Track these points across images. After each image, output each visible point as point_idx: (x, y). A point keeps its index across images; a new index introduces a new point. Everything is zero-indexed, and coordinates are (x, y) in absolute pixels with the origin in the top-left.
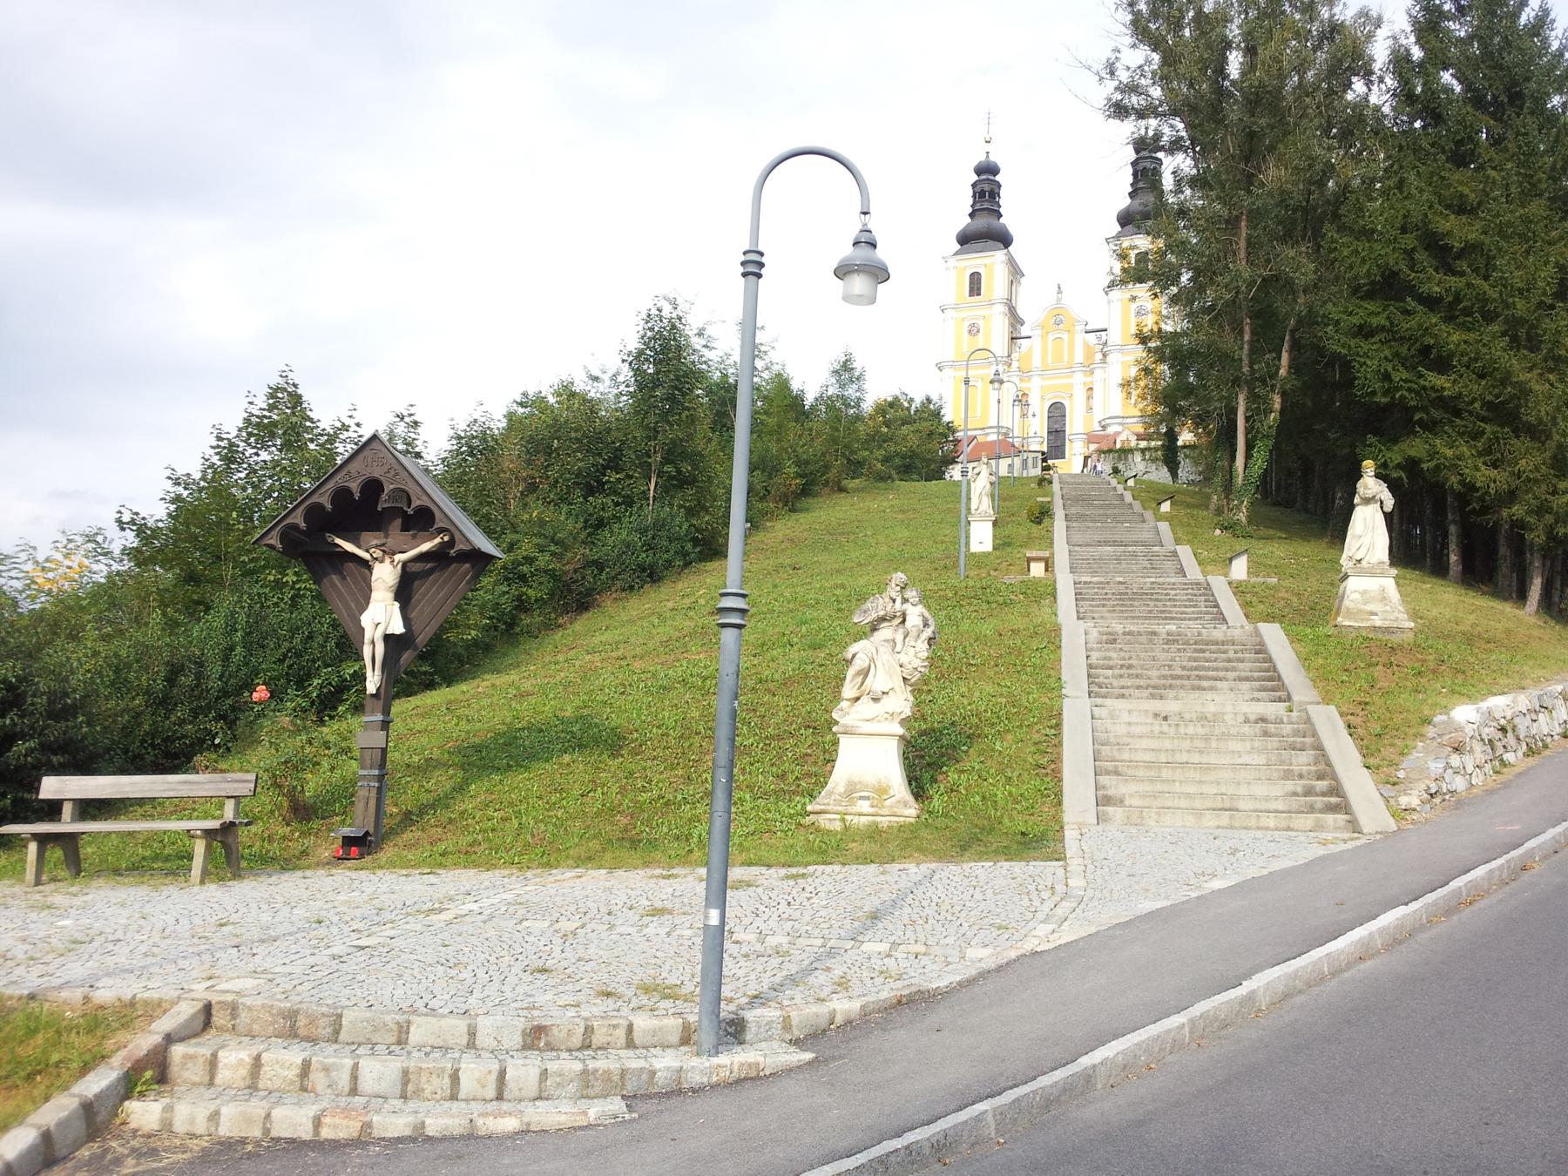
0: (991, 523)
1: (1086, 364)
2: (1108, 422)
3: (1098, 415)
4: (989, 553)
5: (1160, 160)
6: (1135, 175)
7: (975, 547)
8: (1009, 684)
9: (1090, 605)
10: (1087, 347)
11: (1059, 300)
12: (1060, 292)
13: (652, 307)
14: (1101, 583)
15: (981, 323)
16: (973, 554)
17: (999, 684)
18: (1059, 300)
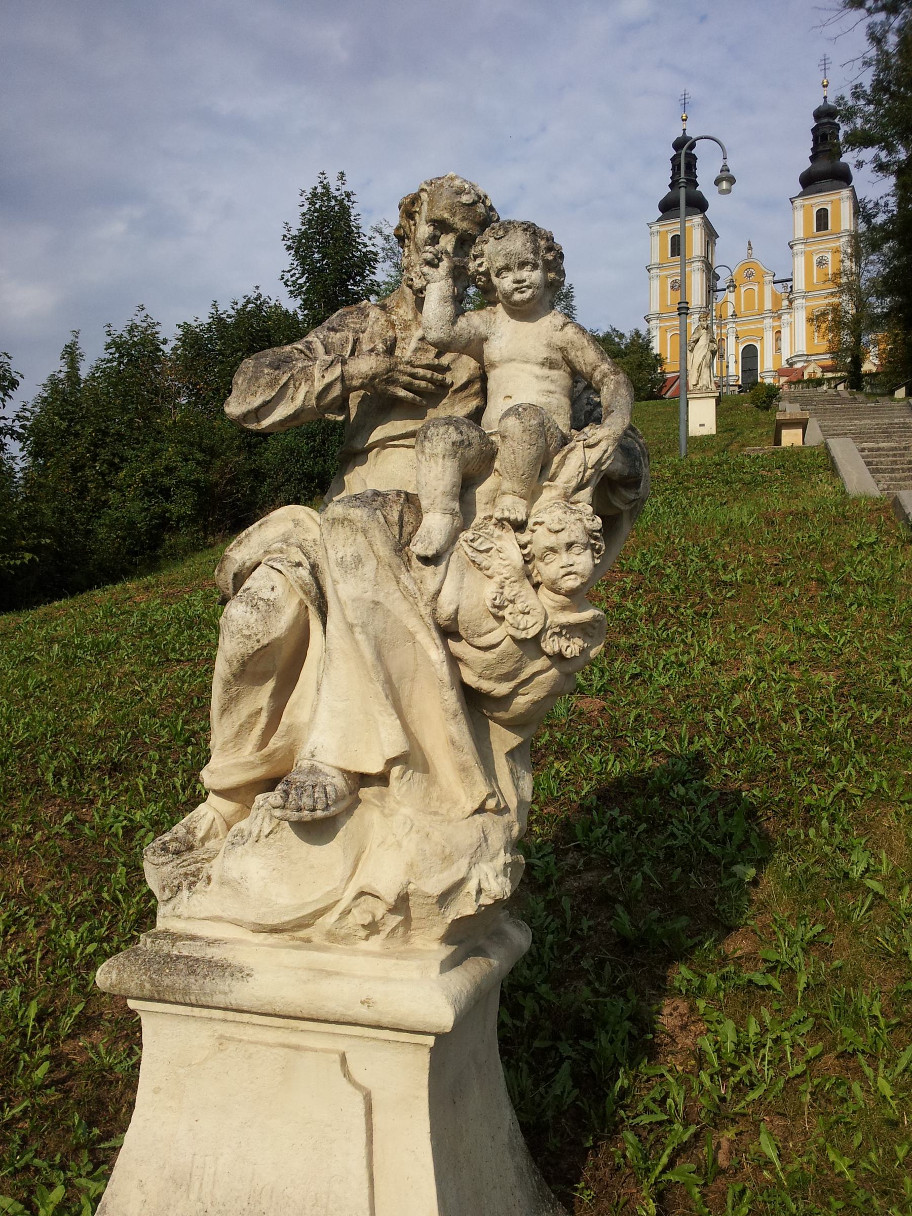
0: (713, 401)
2: (794, 359)
3: (786, 354)
4: (714, 436)
6: (815, 140)
7: (694, 430)
8: (825, 629)
9: (891, 479)
11: (750, 256)
12: (750, 248)
13: (317, 185)
14: (895, 449)
16: (695, 438)
17: (800, 631)
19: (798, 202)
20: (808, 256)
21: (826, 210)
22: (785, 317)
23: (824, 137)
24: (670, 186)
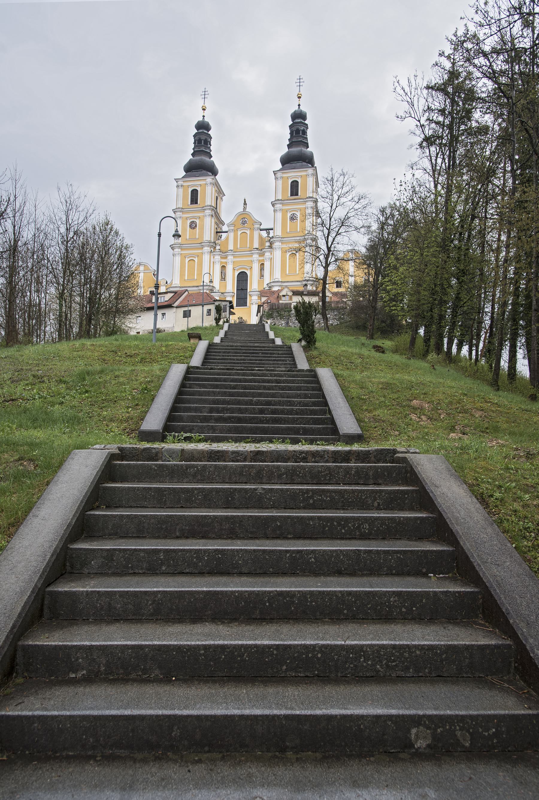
1: (260, 249)
2: (273, 284)
3: (267, 280)
5: (307, 125)
6: (291, 133)
10: (260, 237)
11: (245, 208)
12: (245, 204)
15: (198, 221)
18: (245, 208)
19: (279, 175)
20: (285, 212)
21: (297, 182)
22: (267, 254)
23: (298, 131)
24: (192, 154)
